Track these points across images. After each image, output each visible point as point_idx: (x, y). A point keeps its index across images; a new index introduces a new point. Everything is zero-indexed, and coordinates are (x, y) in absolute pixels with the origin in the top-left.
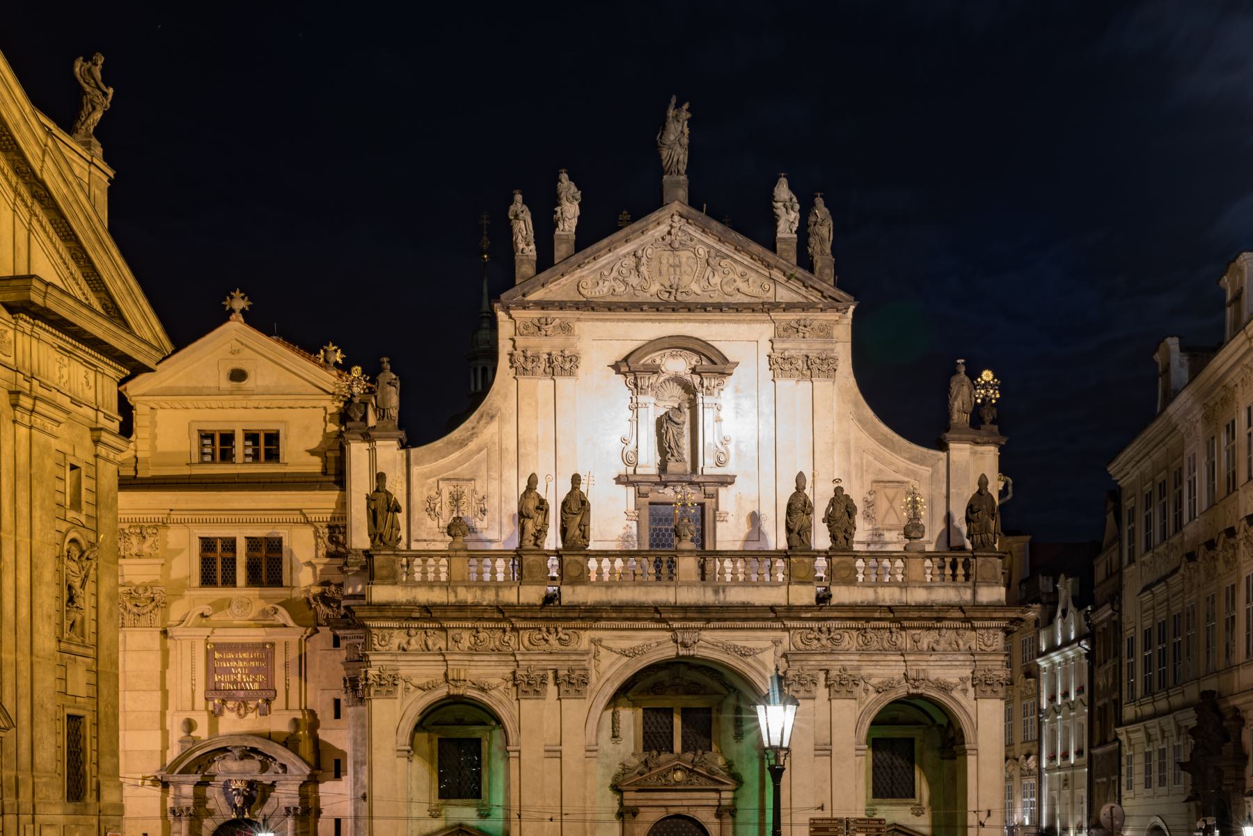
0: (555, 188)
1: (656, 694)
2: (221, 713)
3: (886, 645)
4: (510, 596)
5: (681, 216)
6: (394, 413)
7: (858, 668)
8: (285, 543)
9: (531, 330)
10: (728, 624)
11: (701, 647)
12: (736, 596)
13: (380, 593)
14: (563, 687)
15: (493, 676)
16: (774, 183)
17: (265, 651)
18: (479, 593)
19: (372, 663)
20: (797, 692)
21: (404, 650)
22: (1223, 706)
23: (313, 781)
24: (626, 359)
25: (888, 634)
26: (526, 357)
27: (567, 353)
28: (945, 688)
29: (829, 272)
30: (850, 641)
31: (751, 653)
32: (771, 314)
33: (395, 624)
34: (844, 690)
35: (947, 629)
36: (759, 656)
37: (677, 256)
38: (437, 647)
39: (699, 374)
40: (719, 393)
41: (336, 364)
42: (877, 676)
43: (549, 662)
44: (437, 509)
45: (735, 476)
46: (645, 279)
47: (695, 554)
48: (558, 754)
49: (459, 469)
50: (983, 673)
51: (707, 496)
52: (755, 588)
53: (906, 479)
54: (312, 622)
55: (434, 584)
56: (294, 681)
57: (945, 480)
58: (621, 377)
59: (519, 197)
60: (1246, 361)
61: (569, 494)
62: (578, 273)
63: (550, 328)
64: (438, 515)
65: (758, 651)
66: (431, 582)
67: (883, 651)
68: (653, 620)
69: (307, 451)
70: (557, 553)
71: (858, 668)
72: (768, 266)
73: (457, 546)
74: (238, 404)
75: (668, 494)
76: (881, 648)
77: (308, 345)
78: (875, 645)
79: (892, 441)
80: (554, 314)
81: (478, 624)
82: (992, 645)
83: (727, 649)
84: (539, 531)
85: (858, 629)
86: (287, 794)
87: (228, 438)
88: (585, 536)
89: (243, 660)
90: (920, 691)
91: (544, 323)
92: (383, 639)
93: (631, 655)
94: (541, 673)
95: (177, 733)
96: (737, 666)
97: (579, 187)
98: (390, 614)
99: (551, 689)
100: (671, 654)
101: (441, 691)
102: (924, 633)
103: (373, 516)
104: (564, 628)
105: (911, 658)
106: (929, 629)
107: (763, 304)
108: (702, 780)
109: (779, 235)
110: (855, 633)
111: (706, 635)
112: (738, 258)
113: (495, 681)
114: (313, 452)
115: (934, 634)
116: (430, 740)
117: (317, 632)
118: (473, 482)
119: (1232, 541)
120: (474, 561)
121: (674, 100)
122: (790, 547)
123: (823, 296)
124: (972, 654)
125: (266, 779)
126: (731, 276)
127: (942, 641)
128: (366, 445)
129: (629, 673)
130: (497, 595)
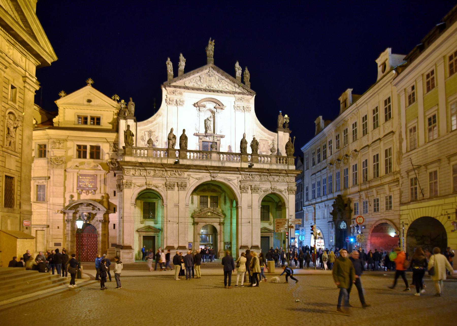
0: (179, 57)
1: (203, 192)
2: (81, 193)
3: (266, 180)
4: (165, 161)
5: (212, 68)
6: (133, 112)
7: (259, 185)
8: (101, 148)
9: (172, 93)
10: (225, 172)
12: (228, 165)
13: (127, 159)
14: (180, 187)
15: (160, 183)
16: (235, 63)
17: (94, 177)
18: (156, 160)
21: (134, 175)
22: (344, 198)
23: (107, 213)
24: (197, 103)
25: (266, 177)
26: (170, 100)
27: (181, 100)
28: (281, 191)
29: (249, 86)
30: (257, 178)
33: (131, 168)
34: (255, 191)
41: (117, 100)
42: (264, 188)
43: (176, 180)
44: (144, 139)
51: (218, 140)
54: (108, 169)
56: (103, 185)
58: (195, 108)
59: (169, 59)
60: (353, 112)
62: (185, 79)
63: (176, 93)
64: (144, 141)
67: (265, 181)
68: (205, 170)
69: (108, 123)
70: (178, 150)
71: (259, 185)
72: (234, 83)
73: (150, 147)
74: (89, 109)
75: (207, 139)
77: (110, 95)
78: (263, 179)
80: (178, 89)
81: (156, 169)
83: (225, 179)
84: (174, 144)
85: (259, 175)
86: (100, 216)
87: (86, 118)
88: (186, 146)
89: (88, 179)
90: (275, 192)
92: (128, 172)
95: (68, 199)
97: (185, 58)
98: (130, 164)
102: (276, 177)
103: (126, 137)
105: (273, 183)
106: (277, 176)
107: (233, 92)
108: (215, 215)
109: (237, 76)
110: (258, 176)
111: (219, 175)
114: (110, 123)
115: (278, 177)
116: (141, 202)
117: (109, 172)
119: (348, 157)
120: (155, 151)
121: (211, 38)
122: (241, 152)
123: (248, 91)
125: (94, 212)
126: (224, 84)
127: (280, 179)
128: (125, 121)
129: (198, 184)
130: (161, 161)
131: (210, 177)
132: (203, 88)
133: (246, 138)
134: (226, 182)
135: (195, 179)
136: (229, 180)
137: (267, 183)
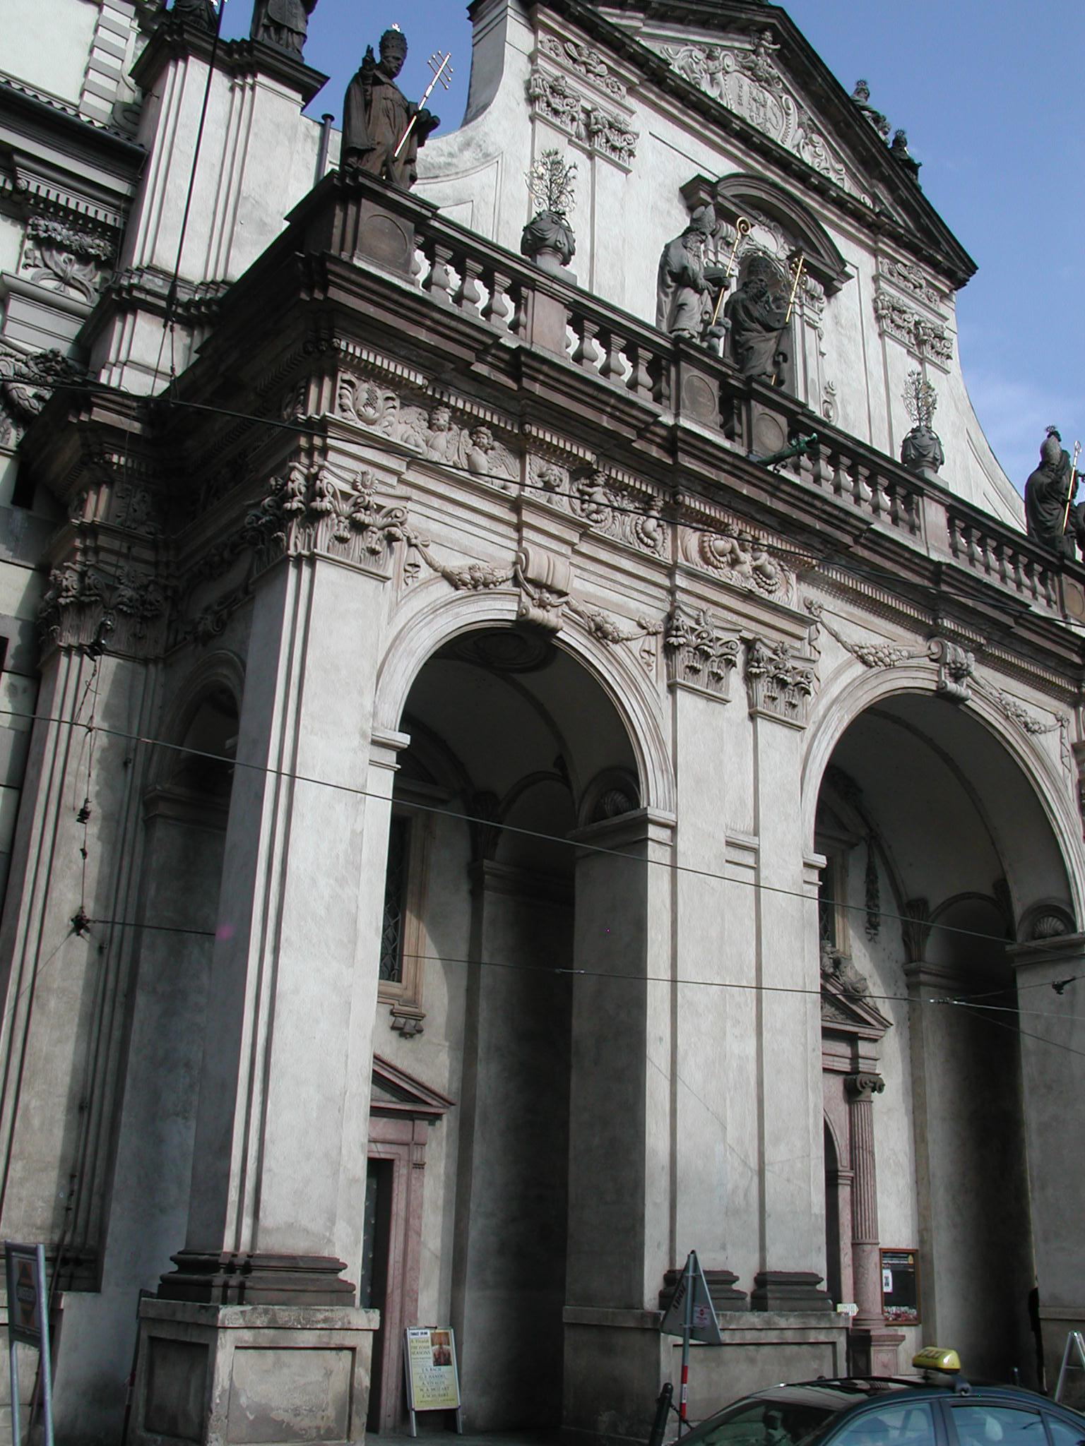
14: (763, 688)
19: (331, 456)
31: (1036, 727)
32: (881, 237)
36: (1042, 737)
48: (749, 859)
83: (1003, 710)
92: (370, 403)
93: (871, 658)
101: (498, 605)
129: (865, 698)
131: (926, 662)
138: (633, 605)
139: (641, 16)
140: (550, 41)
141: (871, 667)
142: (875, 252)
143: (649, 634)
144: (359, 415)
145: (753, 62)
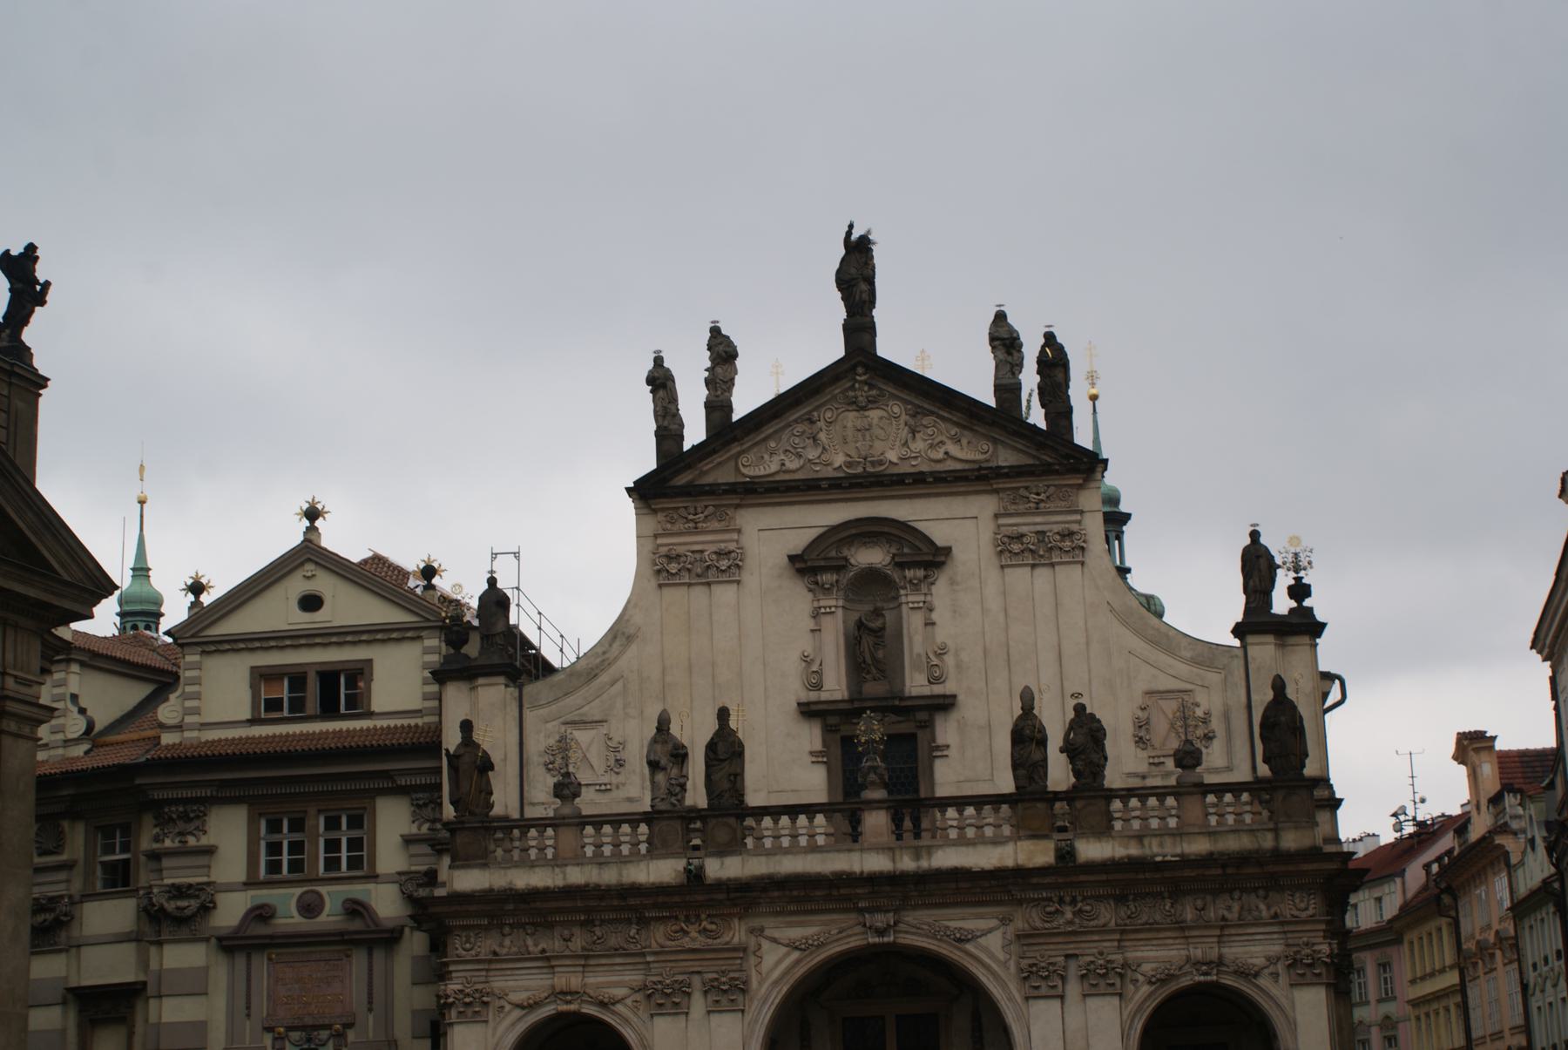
11: (900, 932)
12: (946, 858)
13: (469, 880)
19: (454, 975)
20: (1037, 988)
21: (495, 953)
28: (1249, 974)
30: (1107, 915)
31: (970, 936)
34: (1102, 983)
35: (1243, 890)
36: (982, 941)
37: (868, 416)
38: (540, 948)
39: (901, 566)
40: (929, 590)
45: (954, 696)
46: (824, 448)
47: (886, 805)
49: (586, 709)
50: (1295, 949)
52: (971, 849)
53: (1189, 687)
55: (536, 863)
57: (1243, 683)
61: (717, 734)
65: (979, 934)
66: (532, 861)
67: (1151, 927)
76: (1151, 921)
79: (1167, 636)
82: (1306, 909)
90: (1209, 978)
91: (692, 510)
92: (468, 941)
93: (803, 946)
94: (680, 978)
96: (951, 955)
99: (698, 1004)
100: (858, 943)
102: (1209, 898)
104: (709, 916)
111: (911, 917)
112: (946, 415)
113: (620, 992)
118: (604, 724)
122: (1017, 788)
124: (1282, 923)
129: (800, 971)
131: (859, 929)
132: (829, 473)
133: (1035, 712)
134: (945, 950)
135: (785, 950)
136: (960, 940)
137: (1161, 935)
138: (627, 978)
139: (736, 444)
140: (666, 516)
141: (805, 950)
142: (996, 491)
143: (636, 992)
144: (465, 950)
145: (853, 397)
